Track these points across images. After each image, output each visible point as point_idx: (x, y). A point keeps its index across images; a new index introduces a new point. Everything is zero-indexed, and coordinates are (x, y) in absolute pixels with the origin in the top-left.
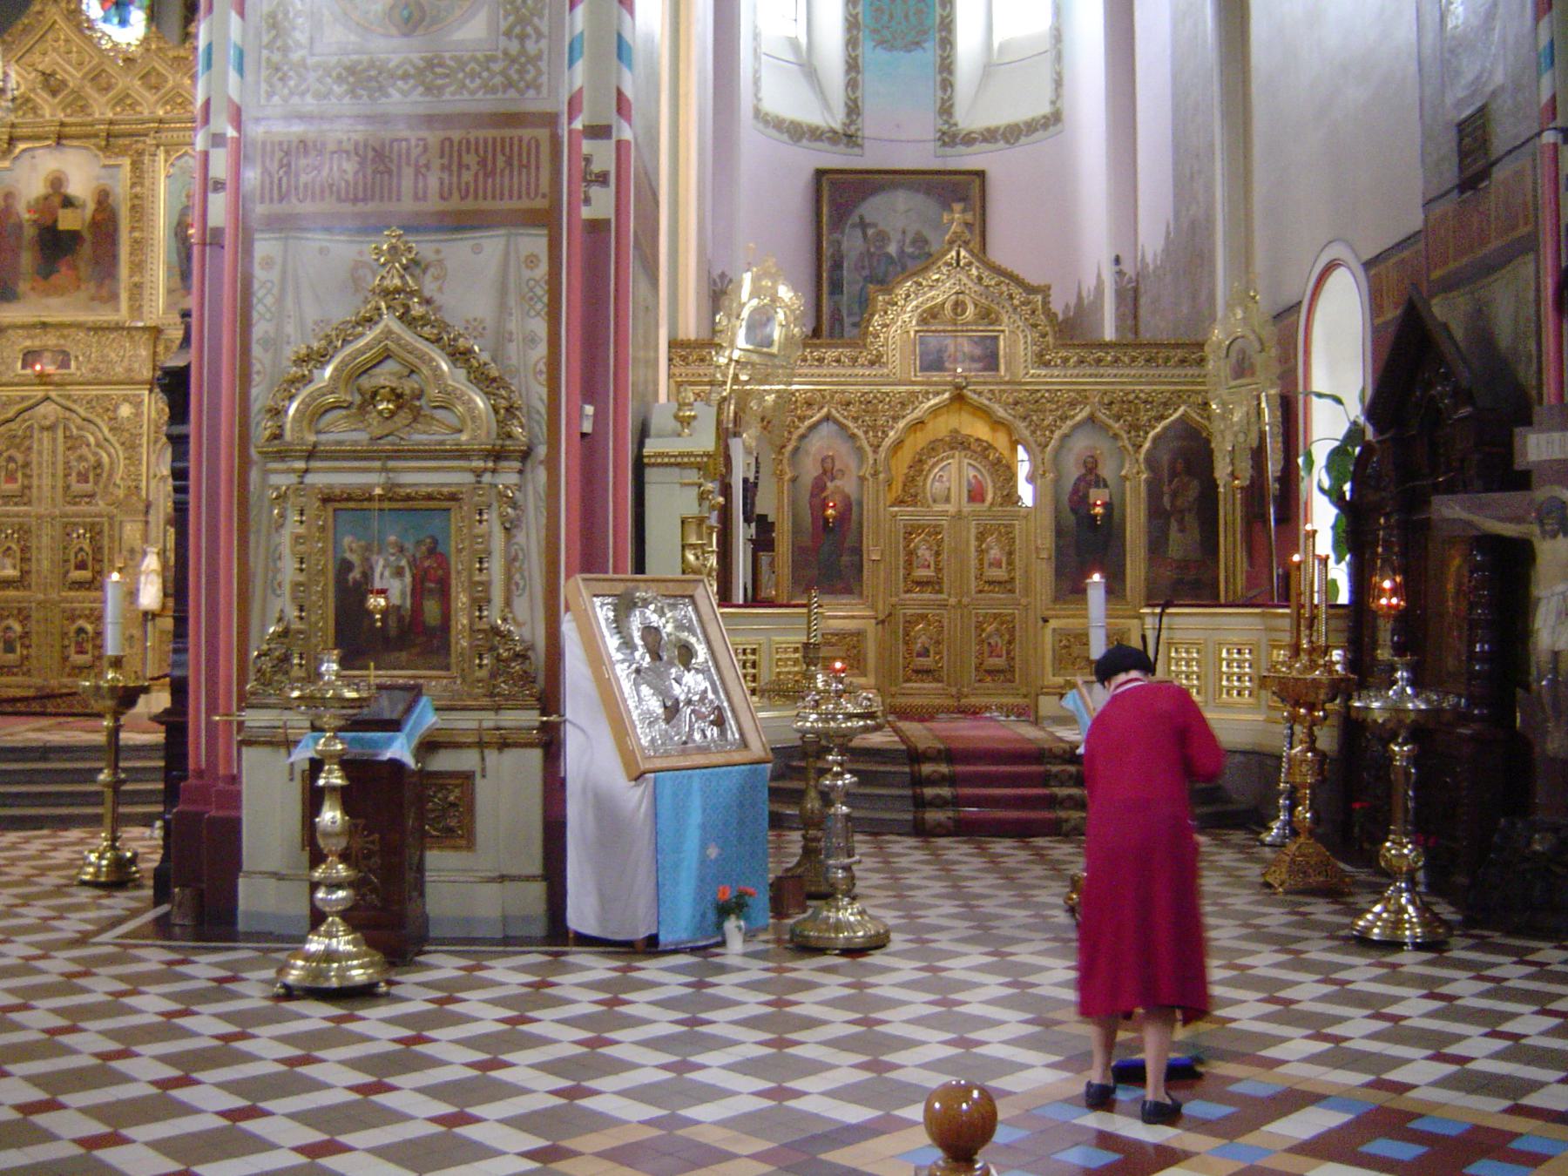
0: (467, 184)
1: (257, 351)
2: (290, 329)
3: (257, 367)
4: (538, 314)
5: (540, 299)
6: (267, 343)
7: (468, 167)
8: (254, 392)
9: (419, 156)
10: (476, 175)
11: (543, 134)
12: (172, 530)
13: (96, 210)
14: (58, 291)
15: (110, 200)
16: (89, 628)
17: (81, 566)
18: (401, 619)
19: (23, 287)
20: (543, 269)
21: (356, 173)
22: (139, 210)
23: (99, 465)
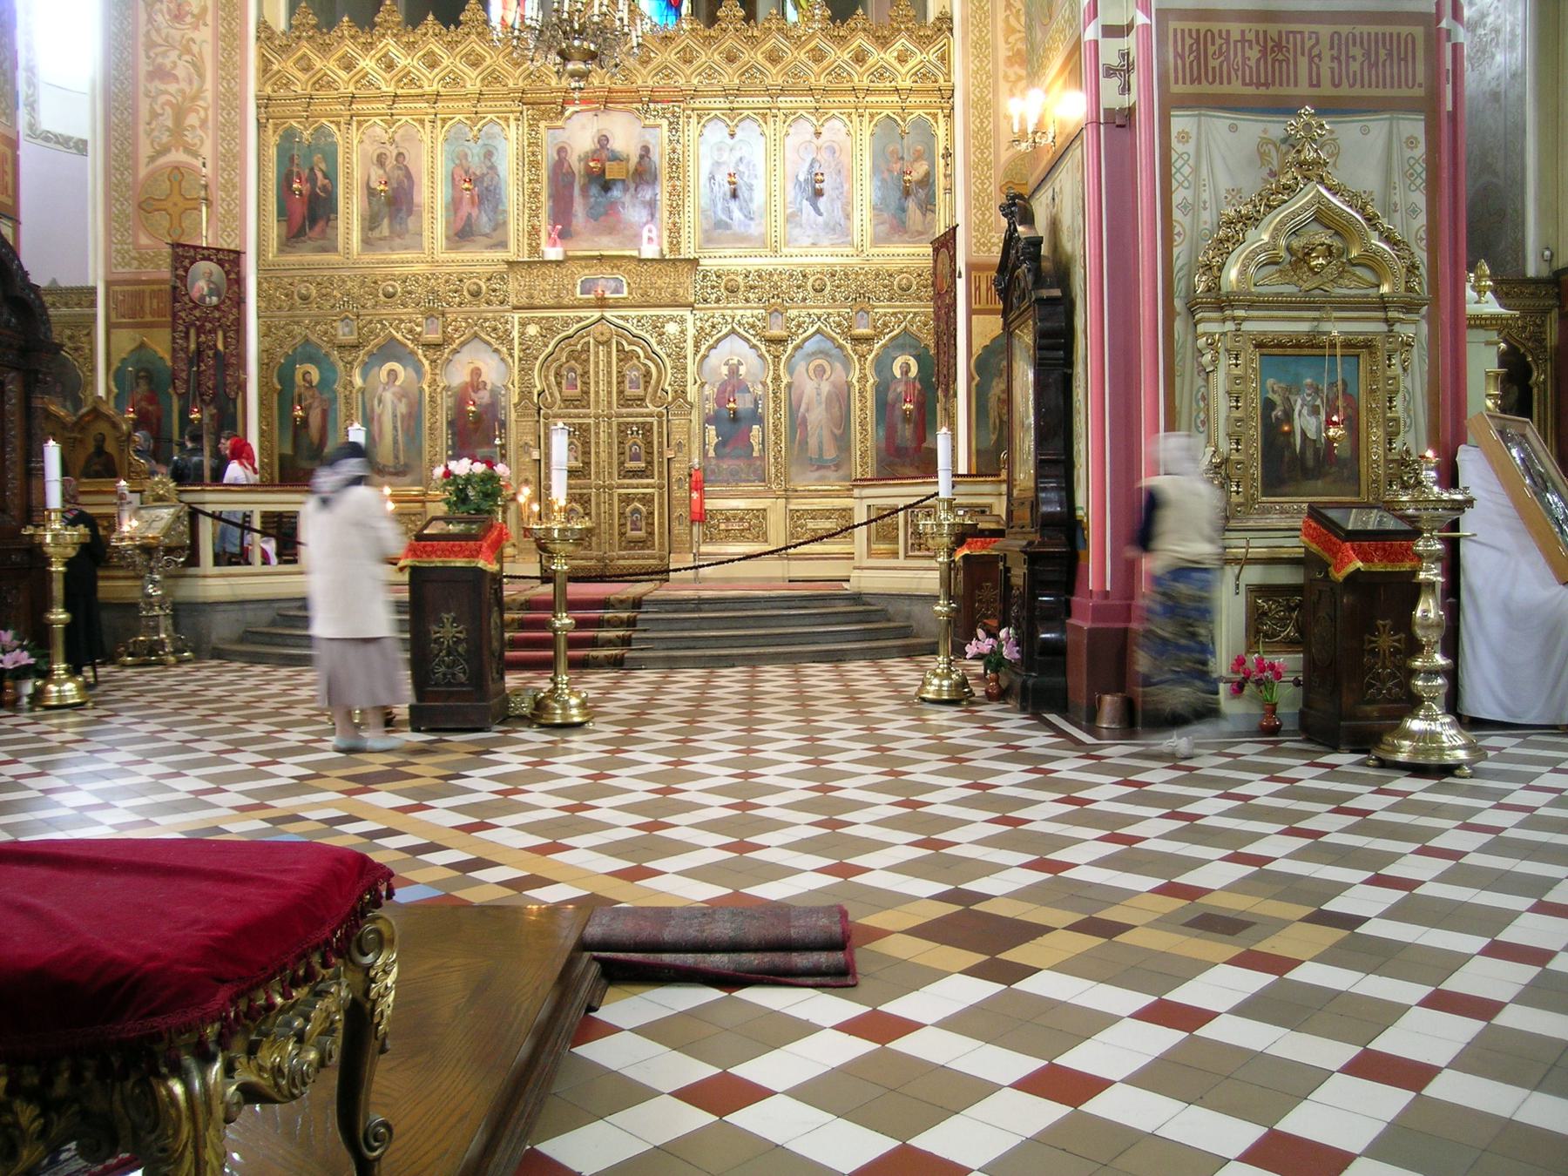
0: (1355, 72)
1: (1177, 215)
2: (1205, 196)
3: (1177, 229)
4: (1418, 188)
5: (1419, 175)
6: (1186, 207)
7: (1354, 58)
8: (1176, 251)
9: (1313, 47)
10: (1362, 64)
11: (1419, 31)
12: (712, 430)
13: (639, 163)
15: (651, 155)
16: (643, 509)
17: (635, 458)
18: (1317, 451)
20: (1420, 150)
21: (1258, 60)
23: (648, 374)
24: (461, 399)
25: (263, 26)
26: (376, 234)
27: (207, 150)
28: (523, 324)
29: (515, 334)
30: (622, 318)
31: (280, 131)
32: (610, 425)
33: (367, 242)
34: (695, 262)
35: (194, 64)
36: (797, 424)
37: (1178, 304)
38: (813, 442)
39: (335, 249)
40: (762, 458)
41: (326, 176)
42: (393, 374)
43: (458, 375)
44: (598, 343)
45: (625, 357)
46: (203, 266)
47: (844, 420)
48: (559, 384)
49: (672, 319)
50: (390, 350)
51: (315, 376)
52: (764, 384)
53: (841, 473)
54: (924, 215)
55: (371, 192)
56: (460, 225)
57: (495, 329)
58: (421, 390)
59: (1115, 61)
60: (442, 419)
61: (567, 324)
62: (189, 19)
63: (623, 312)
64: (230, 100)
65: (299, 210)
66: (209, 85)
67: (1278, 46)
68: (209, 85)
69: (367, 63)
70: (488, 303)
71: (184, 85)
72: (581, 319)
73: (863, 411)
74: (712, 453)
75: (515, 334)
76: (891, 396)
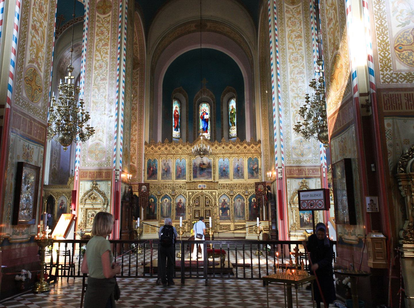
1: (288, 192)
6: (289, 191)
12: (221, 211)
14: (204, 176)
19: (198, 175)
22: (214, 166)
23: (210, 201)
24: (178, 204)
25: (146, 143)
26: (164, 177)
27: (136, 162)
28: (189, 192)
29: (187, 194)
30: (206, 192)
31: (148, 159)
32: (203, 210)
33: (162, 178)
34: (218, 182)
35: (134, 149)
36: (235, 209)
37: (288, 203)
38: (238, 213)
39: (157, 179)
40: (230, 215)
41: (155, 167)
42: (166, 200)
43: (178, 201)
44: (201, 196)
45: (206, 198)
46: (143, 186)
47: (243, 209)
48: (195, 203)
49: (214, 192)
50: (166, 196)
51: (153, 200)
52: (230, 203)
53: (243, 218)
54: (257, 174)
55: (163, 170)
56: (178, 175)
57: (184, 193)
58: (171, 203)
59: (280, 171)
60: (174, 208)
61: (196, 192)
62: (133, 141)
63: (206, 191)
64: (140, 154)
65: (151, 173)
66: (136, 152)
67: (301, 170)
68: (136, 152)
69: (163, 149)
70: (183, 189)
71: (132, 152)
72: (198, 192)
73: (247, 208)
74: (221, 215)
75: (187, 194)
76: (252, 205)
